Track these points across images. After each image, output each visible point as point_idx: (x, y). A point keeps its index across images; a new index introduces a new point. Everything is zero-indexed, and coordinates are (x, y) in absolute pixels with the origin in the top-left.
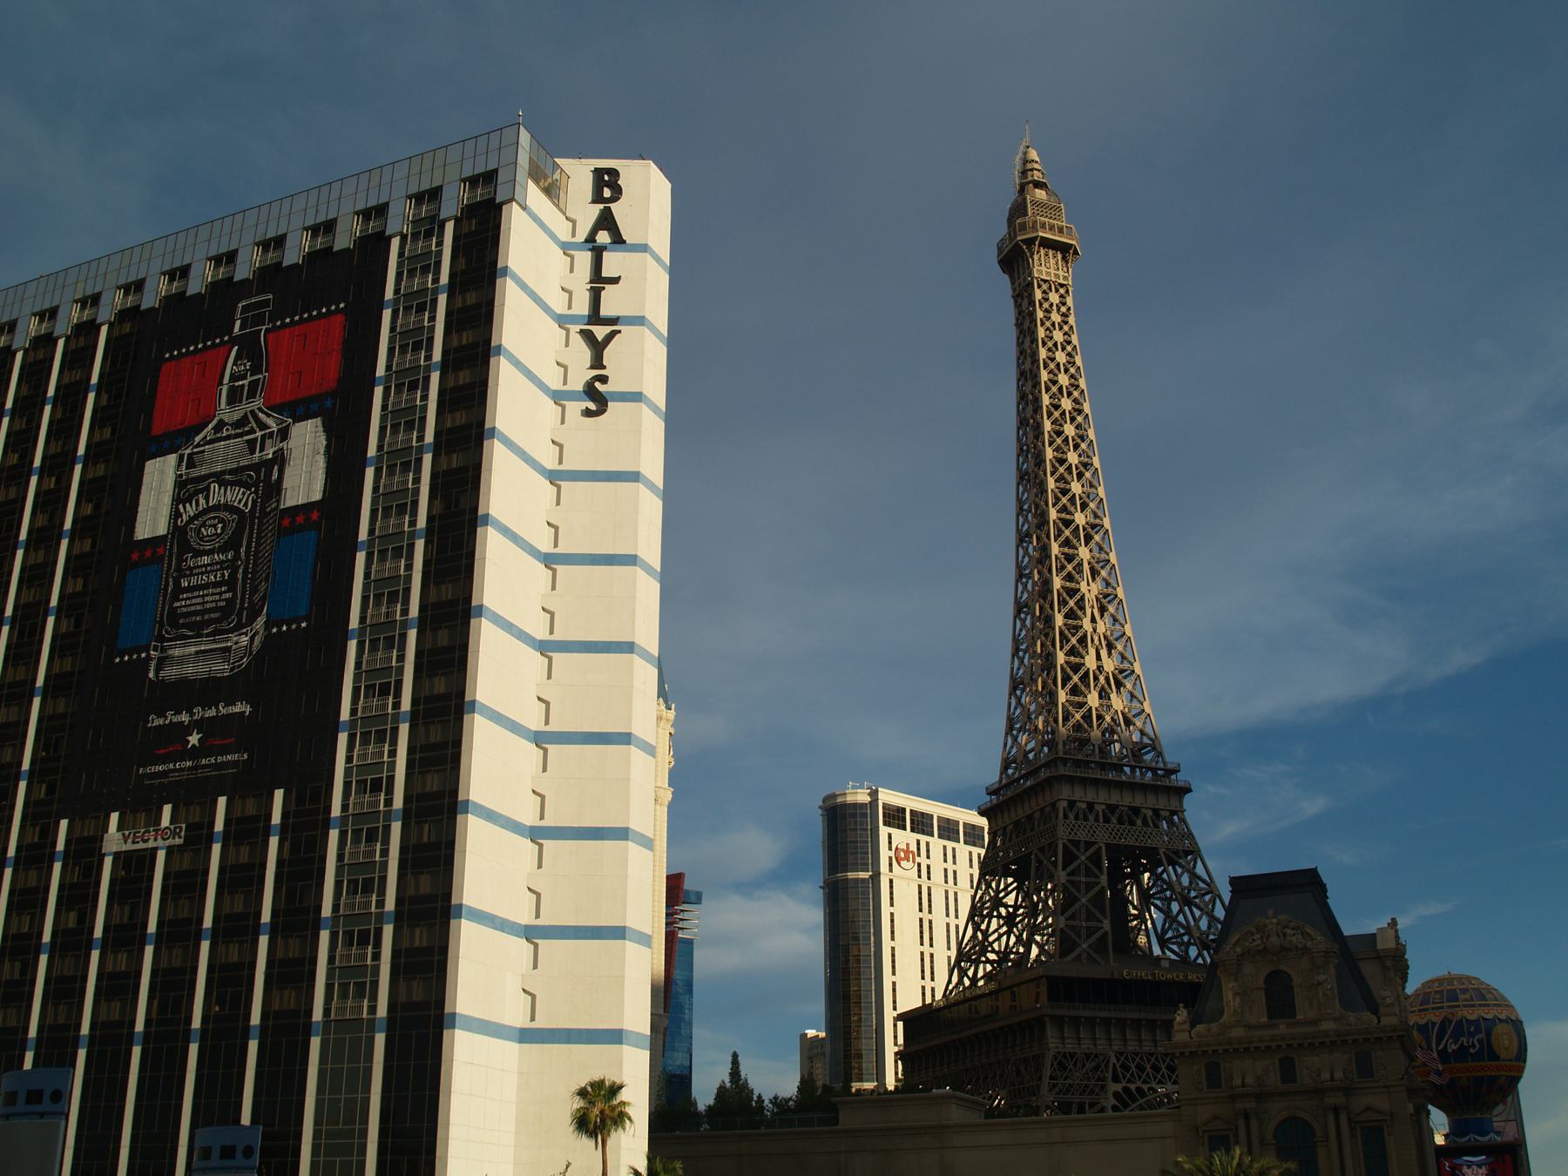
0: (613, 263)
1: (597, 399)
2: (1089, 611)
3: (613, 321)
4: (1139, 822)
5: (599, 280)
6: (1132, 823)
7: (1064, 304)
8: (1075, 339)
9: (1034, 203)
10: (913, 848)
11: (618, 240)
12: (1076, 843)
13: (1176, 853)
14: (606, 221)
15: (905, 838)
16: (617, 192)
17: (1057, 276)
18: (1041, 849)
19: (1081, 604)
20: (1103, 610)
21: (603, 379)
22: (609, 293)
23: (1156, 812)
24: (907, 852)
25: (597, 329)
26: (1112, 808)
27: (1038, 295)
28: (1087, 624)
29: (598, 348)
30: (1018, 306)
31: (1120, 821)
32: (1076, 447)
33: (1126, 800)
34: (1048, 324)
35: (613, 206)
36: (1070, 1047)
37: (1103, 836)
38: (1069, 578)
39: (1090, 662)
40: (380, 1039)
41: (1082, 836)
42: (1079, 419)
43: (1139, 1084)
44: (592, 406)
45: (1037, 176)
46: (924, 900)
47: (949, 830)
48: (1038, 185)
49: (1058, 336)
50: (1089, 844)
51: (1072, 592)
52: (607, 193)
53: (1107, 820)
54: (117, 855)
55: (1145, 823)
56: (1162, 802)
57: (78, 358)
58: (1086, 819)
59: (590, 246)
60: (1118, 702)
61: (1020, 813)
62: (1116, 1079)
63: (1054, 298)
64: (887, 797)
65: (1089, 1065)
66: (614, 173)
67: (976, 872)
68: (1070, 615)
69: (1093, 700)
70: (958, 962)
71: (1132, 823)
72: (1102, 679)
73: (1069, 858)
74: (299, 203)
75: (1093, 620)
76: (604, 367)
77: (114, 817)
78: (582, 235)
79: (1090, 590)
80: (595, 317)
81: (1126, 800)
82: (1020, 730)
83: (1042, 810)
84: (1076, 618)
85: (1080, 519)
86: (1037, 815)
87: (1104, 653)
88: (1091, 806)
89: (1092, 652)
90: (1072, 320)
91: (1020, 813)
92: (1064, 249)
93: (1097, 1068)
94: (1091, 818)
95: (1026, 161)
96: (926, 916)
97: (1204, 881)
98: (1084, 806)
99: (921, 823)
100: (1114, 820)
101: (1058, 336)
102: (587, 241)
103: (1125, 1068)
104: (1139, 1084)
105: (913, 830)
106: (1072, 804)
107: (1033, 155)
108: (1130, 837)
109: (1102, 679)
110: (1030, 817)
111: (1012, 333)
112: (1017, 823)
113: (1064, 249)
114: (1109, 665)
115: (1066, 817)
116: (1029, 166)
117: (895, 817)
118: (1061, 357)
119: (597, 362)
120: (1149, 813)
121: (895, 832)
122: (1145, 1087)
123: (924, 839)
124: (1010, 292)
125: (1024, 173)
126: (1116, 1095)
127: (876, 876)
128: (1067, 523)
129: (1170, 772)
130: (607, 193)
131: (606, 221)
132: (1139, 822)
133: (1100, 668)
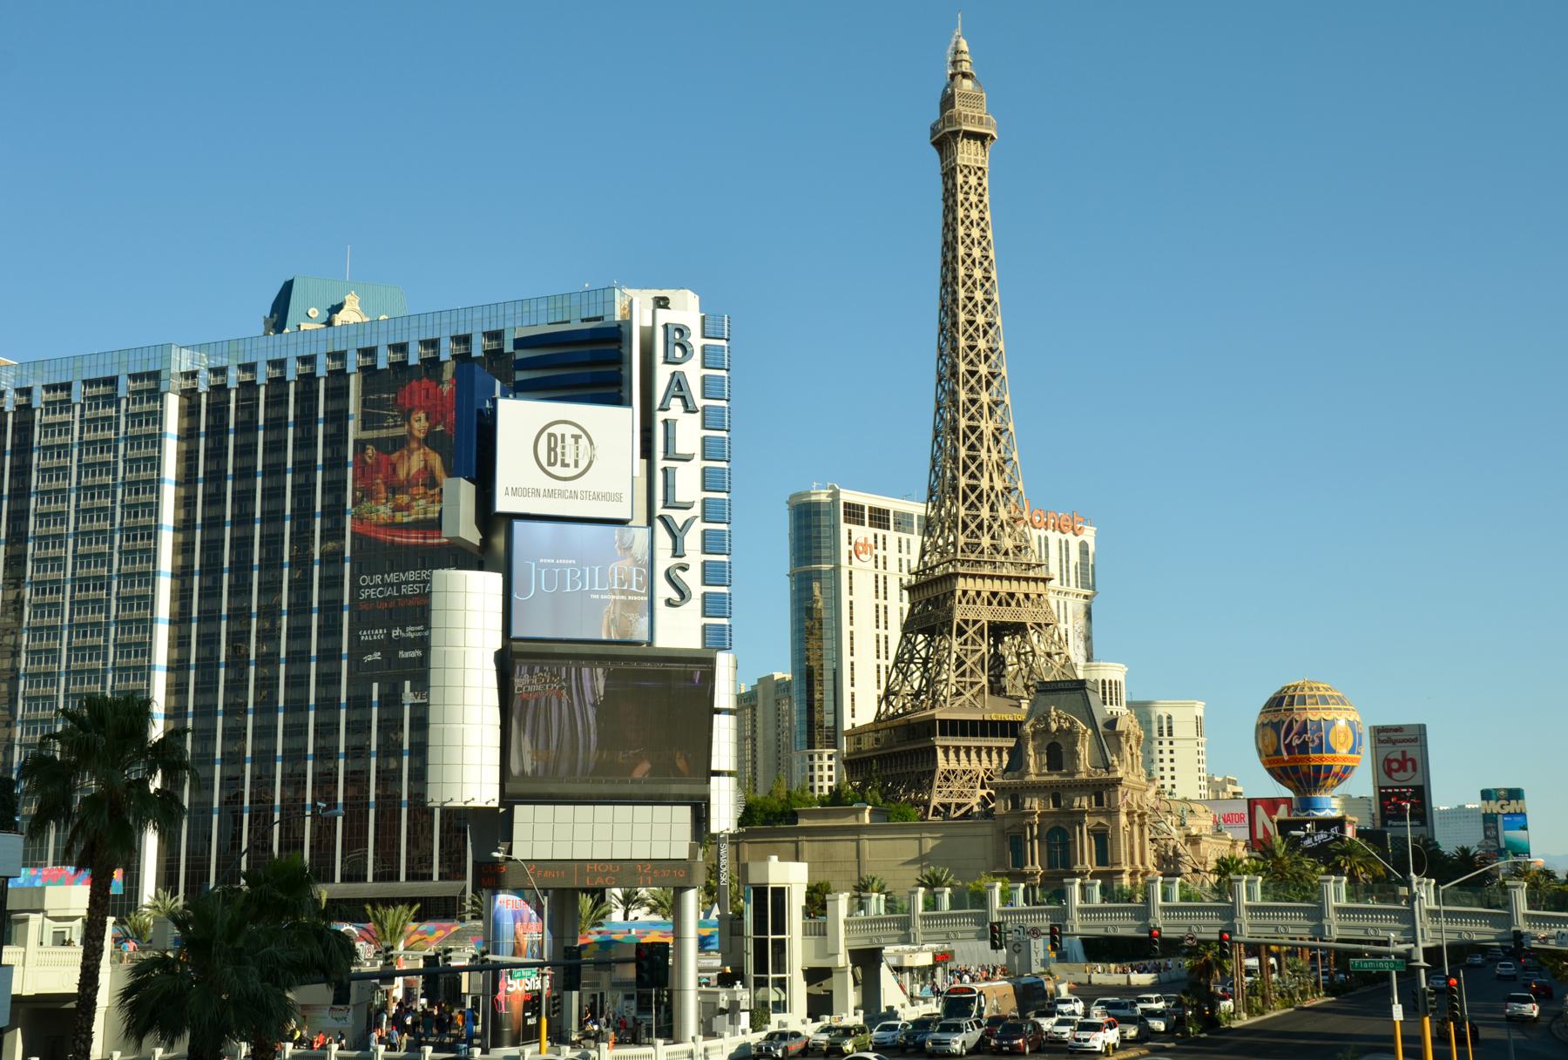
4: (1013, 603)
6: (1009, 604)
8: (987, 216)
9: (964, 96)
10: (871, 541)
13: (1039, 625)
15: (863, 533)
19: (980, 438)
20: (997, 441)
23: (1027, 596)
24: (865, 545)
26: (994, 594)
27: (960, 179)
28: (984, 454)
30: (945, 183)
31: (1000, 604)
32: (984, 308)
33: (1003, 588)
34: (967, 204)
36: (953, 765)
37: (986, 615)
38: (972, 418)
39: (984, 484)
41: (971, 617)
42: (987, 285)
45: (966, 67)
46: (880, 586)
47: (903, 522)
48: (965, 75)
49: (974, 214)
50: (975, 622)
53: (990, 603)
54: (412, 705)
55: (1018, 604)
56: (1032, 588)
57: (338, 390)
60: (1003, 514)
61: (930, 593)
62: (983, 787)
63: (973, 180)
64: (847, 496)
65: (966, 778)
67: (895, 634)
68: (972, 447)
69: (985, 513)
70: (886, 697)
71: (1009, 604)
72: (993, 496)
74: (477, 315)
75: (989, 450)
77: (407, 684)
79: (987, 426)
81: (1003, 588)
85: (983, 369)
87: (995, 476)
88: (978, 593)
89: (986, 475)
90: (986, 199)
91: (930, 593)
92: (982, 138)
95: (957, 52)
96: (881, 602)
99: (880, 518)
100: (995, 602)
101: (974, 214)
105: (871, 525)
106: (965, 593)
107: (964, 45)
108: (1007, 615)
111: (940, 206)
113: (982, 138)
114: (999, 486)
116: (959, 57)
117: (854, 513)
118: (976, 233)
120: (1022, 597)
121: (855, 528)
123: (880, 532)
124: (939, 170)
125: (954, 63)
127: (837, 569)
132: (1013, 603)
133: (992, 488)
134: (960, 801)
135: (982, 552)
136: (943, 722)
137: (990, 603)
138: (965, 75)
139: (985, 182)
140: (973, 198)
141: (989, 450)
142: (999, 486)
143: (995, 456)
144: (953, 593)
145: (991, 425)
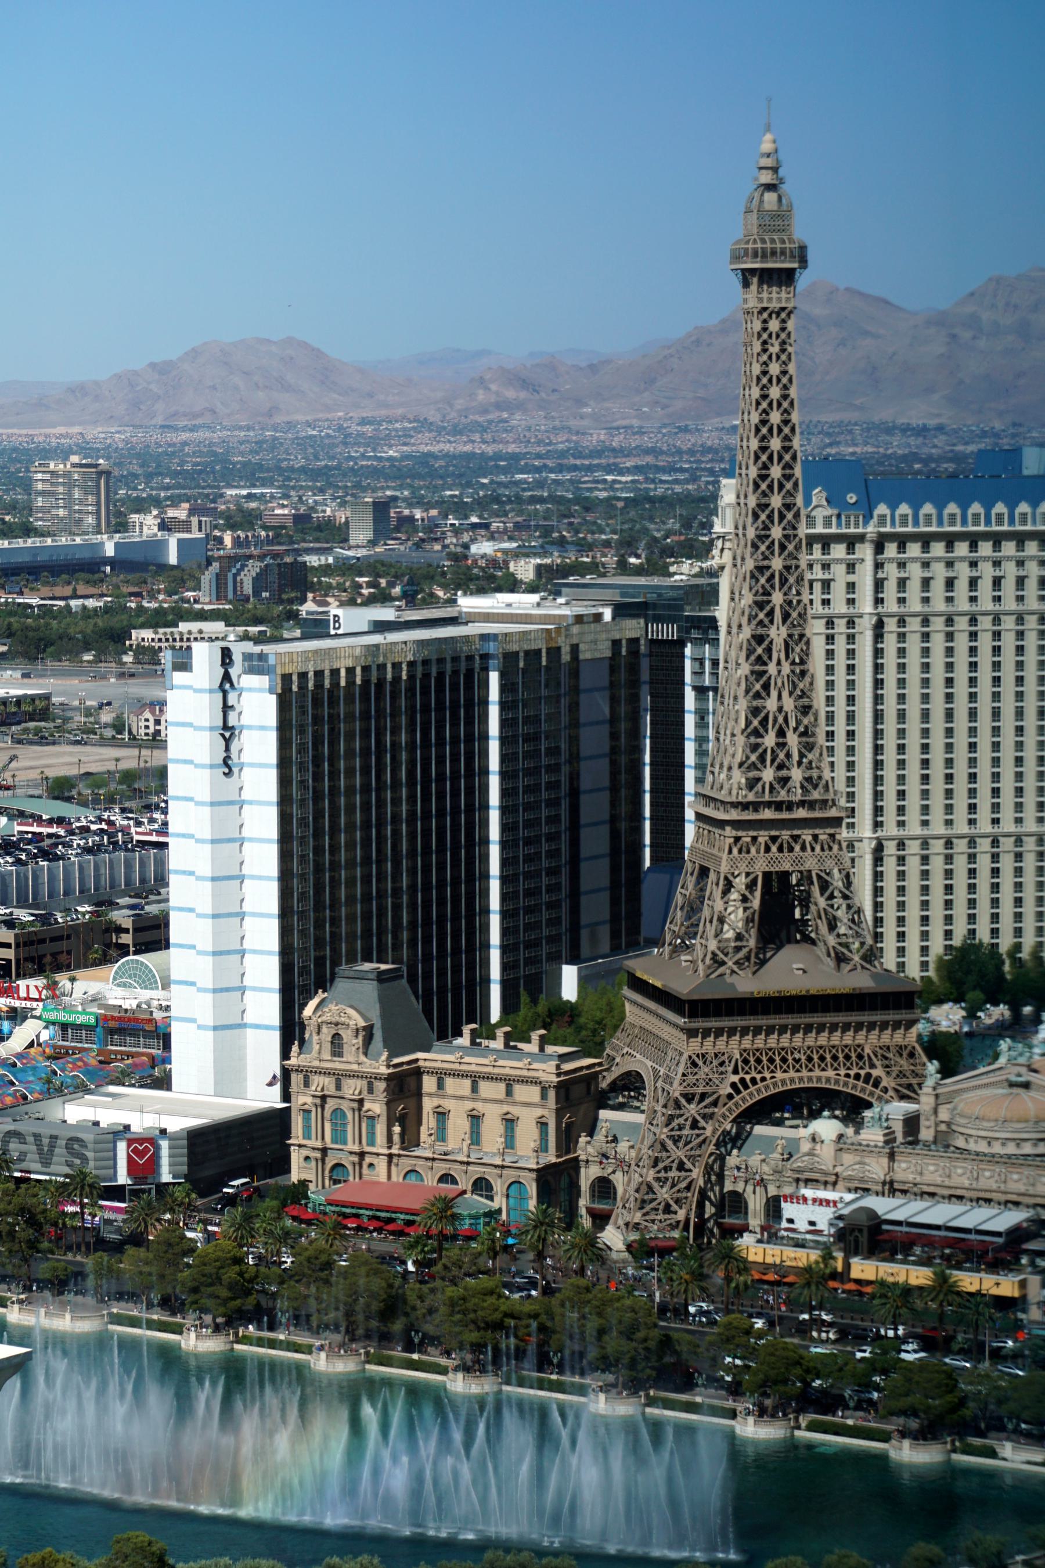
6: (791, 849)
19: (769, 650)
26: (774, 839)
28: (772, 668)
31: (780, 849)
39: (771, 704)
43: (754, 1074)
53: (768, 849)
55: (803, 848)
58: (748, 852)
62: (735, 1072)
69: (770, 740)
75: (779, 663)
84: (765, 664)
87: (785, 694)
88: (754, 839)
89: (774, 694)
93: (722, 1064)
103: (746, 1061)
104: (754, 1074)
109: (781, 720)
115: (730, 852)
122: (758, 1077)
126: (733, 1085)
132: (797, 848)
133: (780, 709)
134: (708, 1089)
137: (768, 849)
141: (779, 663)
143: (786, 668)
145: (784, 631)
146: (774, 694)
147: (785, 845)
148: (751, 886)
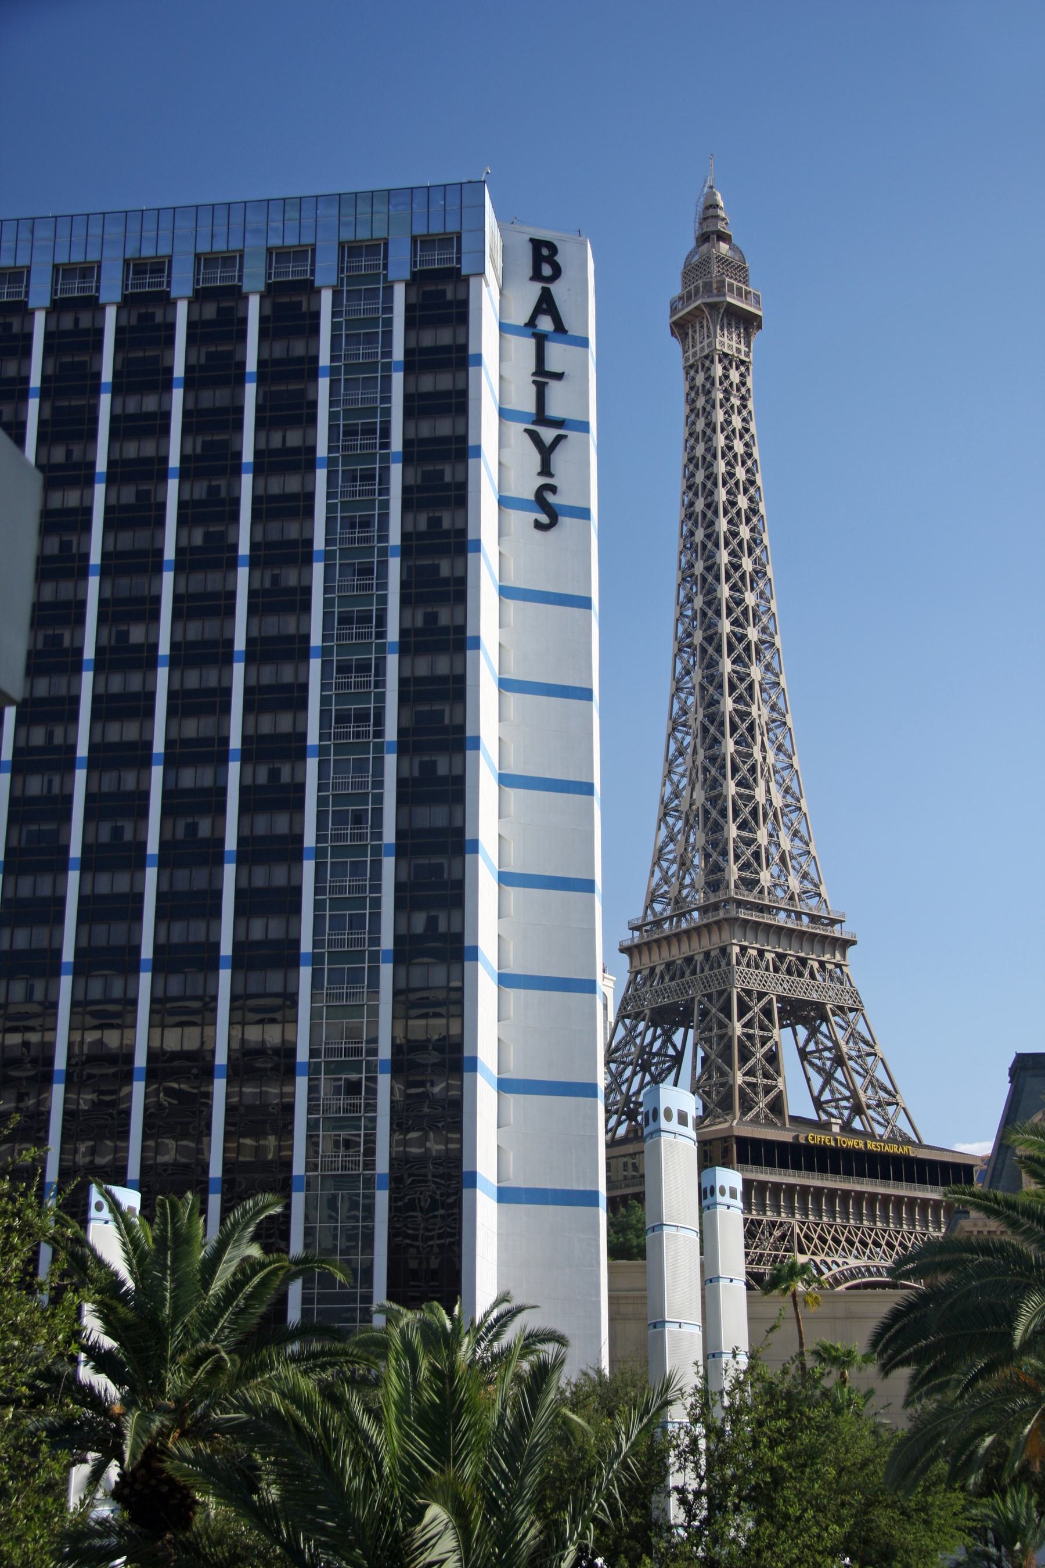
0: (557, 355)
1: (548, 510)
2: (759, 738)
3: (559, 423)
5: (544, 376)
6: (800, 975)
7: (744, 384)
8: (753, 427)
11: (560, 328)
12: (749, 992)
13: (841, 1008)
14: (546, 304)
16: (557, 272)
17: (739, 351)
18: (709, 996)
19: (751, 729)
21: (553, 489)
22: (554, 388)
23: (822, 964)
25: (546, 431)
26: (781, 957)
27: (718, 370)
28: (756, 751)
29: (546, 452)
35: (554, 288)
40: (382, 1199)
41: (755, 987)
43: (823, 1257)
44: (544, 519)
45: (721, 226)
48: (723, 237)
50: (761, 995)
51: (744, 715)
52: (547, 270)
53: (776, 970)
55: (812, 976)
59: (530, 331)
61: (677, 953)
62: (802, 1251)
63: (735, 376)
66: (553, 248)
71: (800, 975)
73: (744, 1009)
76: (551, 475)
78: (520, 316)
79: (760, 712)
80: (541, 418)
82: (672, 862)
83: (707, 954)
85: (753, 634)
86: (699, 958)
88: (761, 953)
90: (750, 405)
93: (783, 1237)
94: (763, 964)
97: (866, 1043)
98: (755, 953)
102: (526, 325)
110: (689, 960)
112: (669, 965)
119: (546, 470)
120: (816, 965)
124: (679, 363)
128: (741, 638)
129: (833, 922)
130: (547, 270)
131: (546, 304)
132: (807, 973)
133: (770, 801)
135: (761, 892)
136: (742, 1141)
138: (723, 237)
139: (749, 381)
140: (736, 402)
142: (778, 801)
144: (724, 951)
146: (762, 783)
147: (794, 969)
148: (767, 1012)
